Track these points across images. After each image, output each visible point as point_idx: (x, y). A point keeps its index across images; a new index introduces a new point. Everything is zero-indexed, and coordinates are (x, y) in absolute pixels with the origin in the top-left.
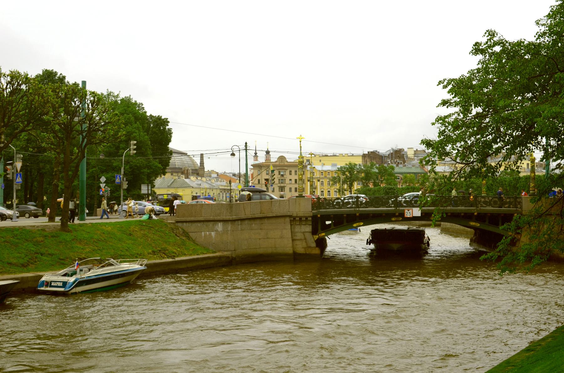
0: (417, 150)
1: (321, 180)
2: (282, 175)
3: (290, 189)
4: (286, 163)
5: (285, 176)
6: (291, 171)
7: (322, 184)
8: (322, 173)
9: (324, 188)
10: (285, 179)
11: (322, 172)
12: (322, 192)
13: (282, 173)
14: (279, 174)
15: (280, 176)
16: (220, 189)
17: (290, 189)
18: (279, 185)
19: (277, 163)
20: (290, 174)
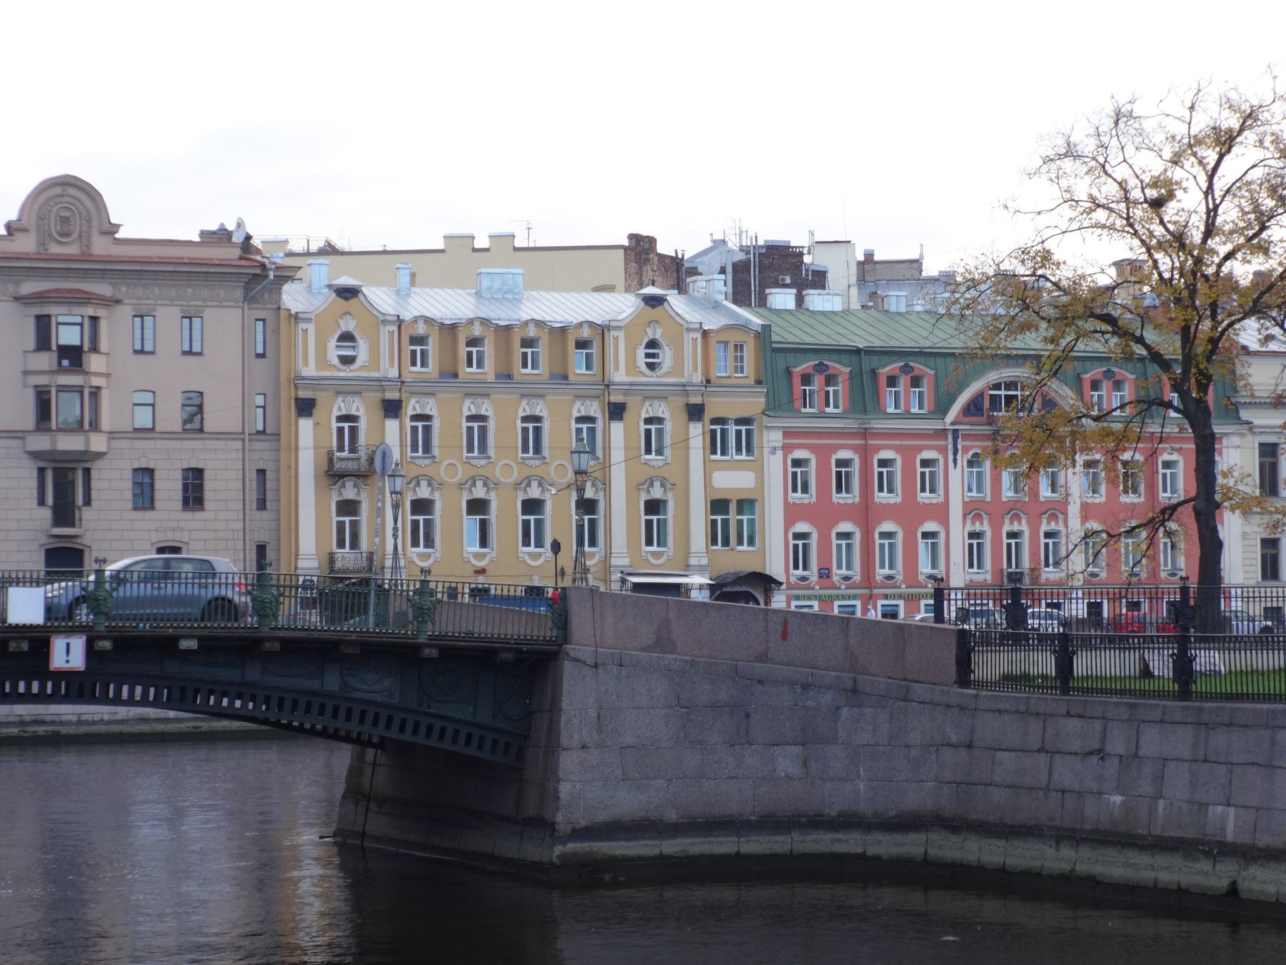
0: (869, 256)
1: (412, 407)
2: (73, 357)
4: (100, 247)
5: (95, 363)
7: (422, 436)
8: (419, 340)
9: (442, 473)
10: (96, 392)
13: (69, 336)
14: (43, 342)
15: (45, 361)
18: (41, 443)
19: (26, 244)
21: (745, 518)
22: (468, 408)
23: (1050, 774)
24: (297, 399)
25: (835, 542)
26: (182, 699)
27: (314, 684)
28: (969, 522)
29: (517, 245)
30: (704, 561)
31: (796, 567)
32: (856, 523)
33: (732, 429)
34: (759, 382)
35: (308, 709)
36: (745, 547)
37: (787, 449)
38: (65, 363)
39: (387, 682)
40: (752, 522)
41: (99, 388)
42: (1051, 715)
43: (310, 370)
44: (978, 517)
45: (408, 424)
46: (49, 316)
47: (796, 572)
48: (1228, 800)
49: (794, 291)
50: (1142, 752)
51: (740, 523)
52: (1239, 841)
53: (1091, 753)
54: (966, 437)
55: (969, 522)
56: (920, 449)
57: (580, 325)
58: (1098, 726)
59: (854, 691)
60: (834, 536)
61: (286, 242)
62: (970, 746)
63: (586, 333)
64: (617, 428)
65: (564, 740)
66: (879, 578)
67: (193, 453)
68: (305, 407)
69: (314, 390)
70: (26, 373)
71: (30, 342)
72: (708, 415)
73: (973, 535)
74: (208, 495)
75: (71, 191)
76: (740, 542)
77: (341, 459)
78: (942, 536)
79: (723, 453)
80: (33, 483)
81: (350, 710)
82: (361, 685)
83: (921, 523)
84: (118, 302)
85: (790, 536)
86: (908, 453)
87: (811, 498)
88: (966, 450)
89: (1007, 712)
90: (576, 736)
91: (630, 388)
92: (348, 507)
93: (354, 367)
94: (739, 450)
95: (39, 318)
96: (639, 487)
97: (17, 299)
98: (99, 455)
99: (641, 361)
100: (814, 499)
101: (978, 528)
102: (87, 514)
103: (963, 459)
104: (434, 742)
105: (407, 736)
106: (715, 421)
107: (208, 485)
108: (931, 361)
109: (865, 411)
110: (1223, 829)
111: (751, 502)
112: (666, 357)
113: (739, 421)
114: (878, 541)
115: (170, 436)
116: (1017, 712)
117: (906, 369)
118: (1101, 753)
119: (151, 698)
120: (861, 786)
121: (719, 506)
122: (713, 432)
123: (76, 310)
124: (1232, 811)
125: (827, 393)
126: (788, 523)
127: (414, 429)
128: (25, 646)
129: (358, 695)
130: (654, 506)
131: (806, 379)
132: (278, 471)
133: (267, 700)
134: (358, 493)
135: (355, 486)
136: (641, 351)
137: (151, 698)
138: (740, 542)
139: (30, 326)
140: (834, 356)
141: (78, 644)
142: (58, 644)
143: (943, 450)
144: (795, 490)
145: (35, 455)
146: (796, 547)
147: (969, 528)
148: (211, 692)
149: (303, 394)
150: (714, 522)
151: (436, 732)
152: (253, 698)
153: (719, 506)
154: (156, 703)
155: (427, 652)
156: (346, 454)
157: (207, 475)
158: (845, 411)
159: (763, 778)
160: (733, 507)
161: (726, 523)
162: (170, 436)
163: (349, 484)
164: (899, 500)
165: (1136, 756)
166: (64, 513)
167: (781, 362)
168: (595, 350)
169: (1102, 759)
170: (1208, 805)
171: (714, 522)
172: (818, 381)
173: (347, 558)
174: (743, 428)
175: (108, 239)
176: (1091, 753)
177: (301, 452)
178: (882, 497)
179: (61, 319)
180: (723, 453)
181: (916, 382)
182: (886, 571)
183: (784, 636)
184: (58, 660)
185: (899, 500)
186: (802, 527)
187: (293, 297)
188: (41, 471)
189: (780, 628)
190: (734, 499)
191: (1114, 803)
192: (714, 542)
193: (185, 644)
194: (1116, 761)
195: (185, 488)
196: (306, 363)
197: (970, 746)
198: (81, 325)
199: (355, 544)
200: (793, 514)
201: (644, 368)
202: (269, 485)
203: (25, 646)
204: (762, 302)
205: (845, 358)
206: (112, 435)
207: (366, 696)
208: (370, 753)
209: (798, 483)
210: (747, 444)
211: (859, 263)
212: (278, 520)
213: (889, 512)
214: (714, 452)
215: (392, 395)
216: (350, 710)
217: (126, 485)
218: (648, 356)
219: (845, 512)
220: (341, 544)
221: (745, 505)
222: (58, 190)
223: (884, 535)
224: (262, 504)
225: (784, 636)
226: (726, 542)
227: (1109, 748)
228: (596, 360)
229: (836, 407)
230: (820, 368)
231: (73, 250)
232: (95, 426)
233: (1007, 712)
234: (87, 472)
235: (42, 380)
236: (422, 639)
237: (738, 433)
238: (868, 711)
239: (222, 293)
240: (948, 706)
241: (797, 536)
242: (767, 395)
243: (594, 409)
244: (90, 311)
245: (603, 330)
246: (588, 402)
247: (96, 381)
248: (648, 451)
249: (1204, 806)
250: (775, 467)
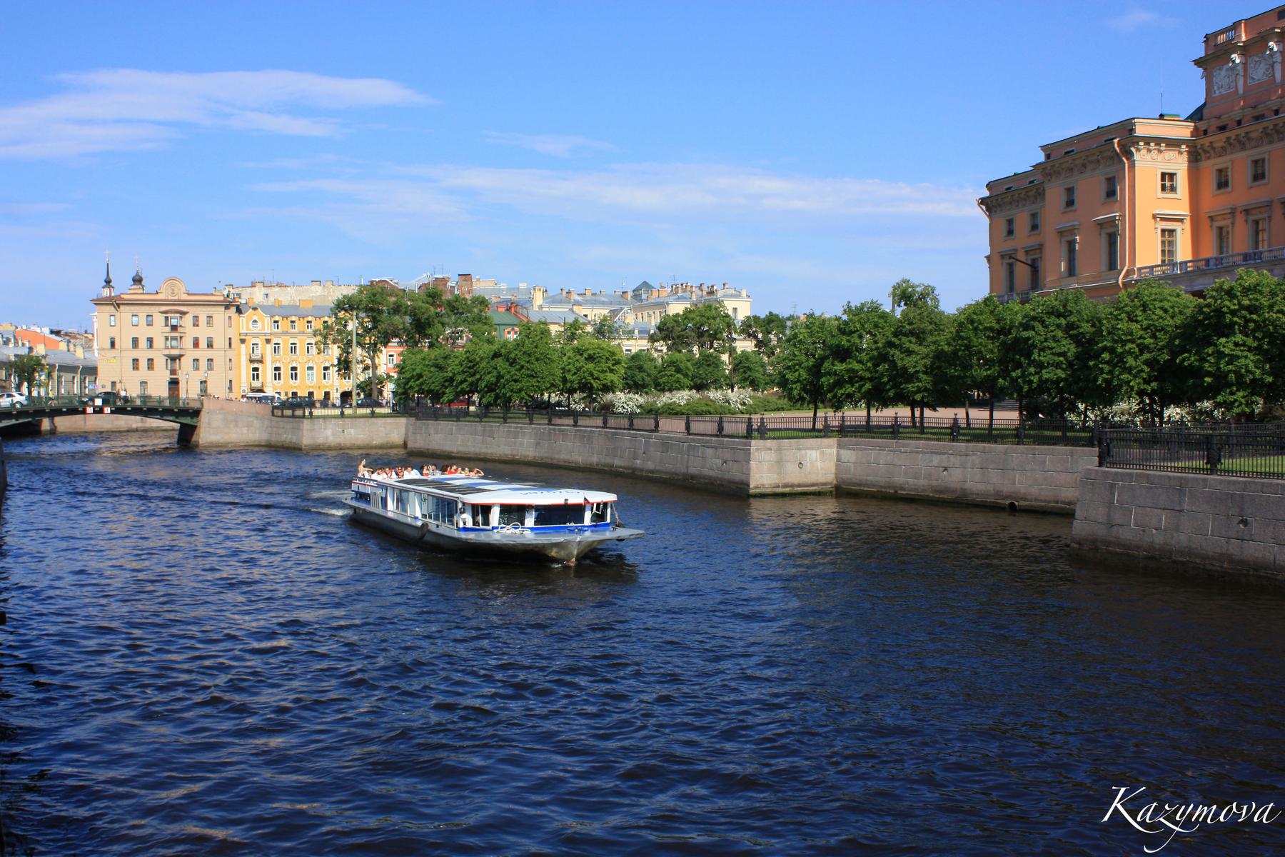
1: (275, 340)
2: (174, 328)
6: (196, 318)
12: (277, 369)
13: (174, 322)
14: (167, 326)
18: (167, 352)
20: (196, 325)
22: (292, 341)
67: (210, 354)
68: (243, 341)
71: (164, 324)
92: (256, 369)
102: (180, 372)
139: (164, 319)
145: (165, 355)
166: (173, 372)
173: (256, 384)
220: (254, 379)
231: (176, 298)
235: (167, 335)
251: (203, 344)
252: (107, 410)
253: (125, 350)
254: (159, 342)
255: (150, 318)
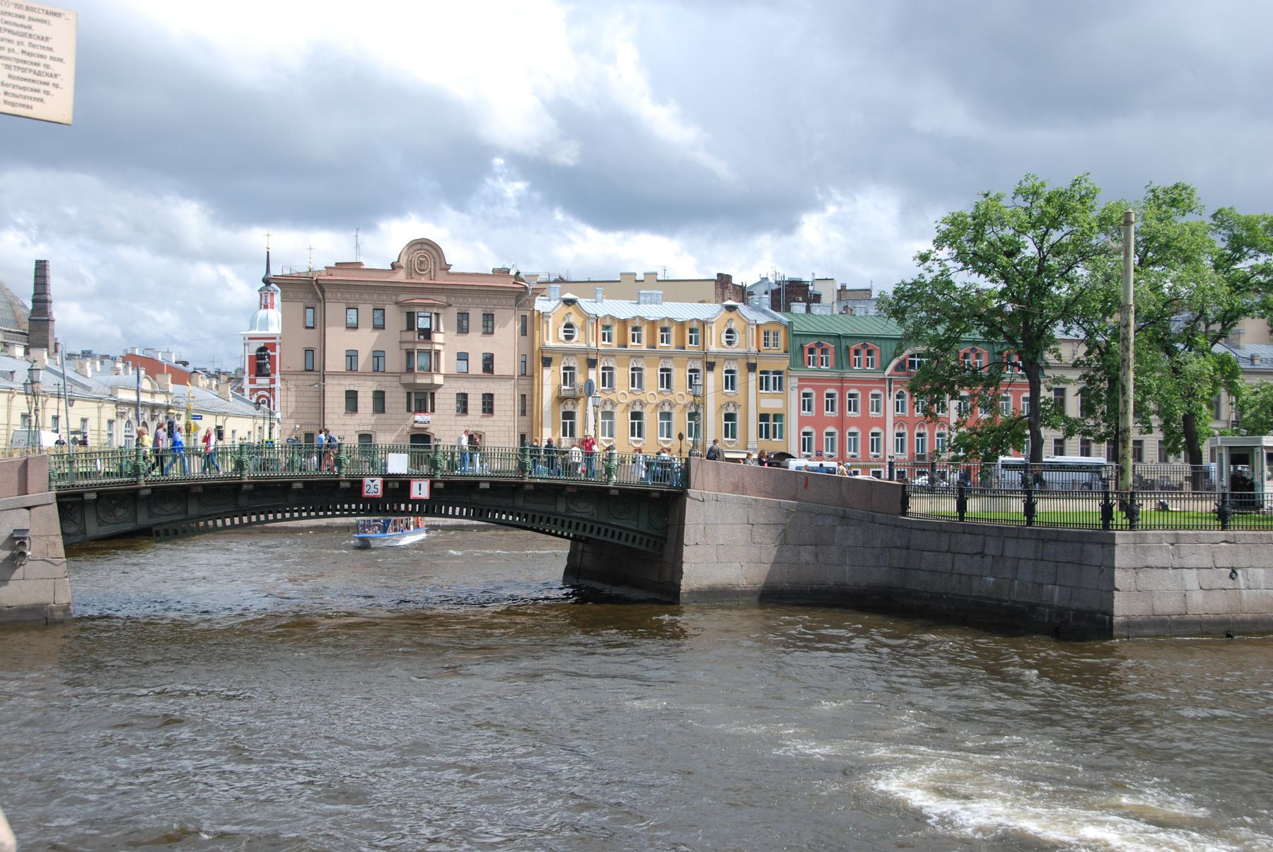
0: (843, 287)
3: (463, 400)
5: (437, 338)
6: (463, 316)
10: (438, 353)
11: (606, 326)
13: (423, 323)
14: (411, 325)
16: (118, 404)
17: (463, 400)
18: (408, 379)
19: (401, 276)
21: (777, 424)
23: (953, 565)
24: (542, 358)
25: (825, 437)
26: (481, 514)
27: (552, 508)
28: (896, 428)
29: (658, 279)
30: (756, 446)
31: (804, 450)
32: (836, 427)
33: (771, 377)
34: (786, 352)
35: (548, 521)
36: (777, 439)
37: (800, 388)
38: (422, 337)
39: (591, 508)
40: (781, 426)
41: (439, 351)
42: (954, 532)
43: (550, 343)
44: (902, 425)
45: (601, 372)
46: (413, 313)
47: (804, 453)
48: (1055, 582)
49: (805, 304)
50: (1006, 554)
51: (775, 426)
52: (1061, 605)
53: (976, 554)
54: (895, 383)
55: (896, 428)
56: (872, 388)
57: (692, 320)
58: (980, 538)
59: (843, 517)
60: (824, 434)
61: (538, 276)
62: (908, 548)
63: (695, 325)
64: (711, 377)
65: (686, 541)
66: (848, 457)
68: (547, 362)
69: (552, 353)
70: (401, 342)
71: (405, 328)
72: (759, 369)
73: (899, 435)
74: (496, 408)
75: (426, 247)
76: (775, 437)
77: (565, 390)
78: (882, 435)
79: (766, 389)
80: (405, 400)
81: (570, 522)
82: (576, 509)
83: (871, 428)
84: (450, 305)
85: (801, 434)
86: (865, 391)
87: (812, 414)
88: (896, 389)
89: (929, 530)
90: (692, 539)
91: (717, 355)
92: (569, 415)
93: (573, 341)
94: (775, 389)
95: (408, 313)
96: (721, 407)
97: (396, 303)
98: (439, 386)
99: (724, 340)
100: (814, 414)
101: (901, 431)
103: (894, 395)
104: (615, 540)
105: (601, 537)
106: (762, 372)
107: (495, 402)
108: (878, 342)
109: (842, 368)
110: (1052, 597)
111: (781, 416)
112: (738, 338)
113: (775, 373)
114: (848, 437)
115: (477, 377)
116: (935, 530)
117: (865, 346)
118: (982, 554)
119: (464, 514)
120: (847, 568)
121: (764, 417)
122: (761, 378)
123: (428, 309)
124: (1057, 588)
125: (822, 358)
126: (801, 426)
127: (604, 375)
128: (397, 485)
129: (574, 514)
130: (730, 417)
131: (811, 351)
132: (532, 395)
133: (526, 516)
134: (574, 408)
135: (572, 404)
136: (724, 335)
137: (464, 514)
138: (775, 437)
139: (405, 316)
140: (827, 339)
141: (426, 484)
142: (415, 485)
143: (883, 390)
144: (804, 409)
145: (405, 385)
146: (804, 439)
147: (897, 431)
148: (496, 511)
149: (545, 355)
150: (761, 426)
151: (617, 535)
152: (519, 515)
153: (764, 417)
154: (467, 517)
155: (613, 492)
156: (567, 387)
157: (495, 397)
158: (832, 368)
159: (794, 563)
160: (771, 418)
161: (767, 426)
162: (477, 377)
163: (569, 403)
164: (859, 415)
165: (1002, 556)
167: (798, 341)
168: (700, 334)
169: (983, 557)
170: (1043, 584)
171: (761, 426)
172: (818, 351)
174: (777, 376)
175: (445, 272)
176: (976, 554)
177: (544, 387)
178: (850, 414)
179: (420, 314)
180: (766, 389)
181: (869, 353)
182: (852, 453)
183: (806, 486)
184: (415, 493)
185: (859, 415)
186: (807, 429)
187: (540, 305)
188: (409, 394)
189: (804, 482)
190: (772, 413)
191: (989, 582)
192: (761, 436)
193: (482, 486)
194: (990, 559)
195: (484, 404)
196: (548, 339)
197: (908, 548)
198: (431, 317)
199: (572, 434)
200: (802, 421)
201: (725, 344)
202: (527, 403)
203: (397, 485)
204: (788, 309)
205: (832, 340)
206: (446, 376)
207: (579, 515)
208: (580, 546)
209: (806, 406)
210: (779, 385)
211: (838, 291)
212: (532, 421)
213: (854, 421)
214: (761, 389)
215: (593, 357)
216: (570, 522)
217: (453, 404)
218: (727, 337)
219: (830, 421)
221: (777, 417)
222: (419, 246)
223: (851, 434)
224: (523, 413)
225: (806, 486)
226: (767, 437)
227: (986, 552)
228: (700, 339)
229: (827, 365)
230: (819, 344)
232: (438, 370)
233: (929, 530)
234: (433, 394)
235: (409, 346)
236: (611, 485)
237: (775, 378)
238: (851, 528)
239: (504, 301)
240: (896, 526)
241: (805, 434)
242: (790, 359)
243: (698, 365)
244: (435, 311)
245: (704, 323)
246: (695, 362)
247: (437, 347)
248: (727, 388)
249: (1041, 585)
250: (794, 398)
251: (476, 366)
252: (421, 490)
253: (335, 374)
254: (395, 361)
255: (378, 314)
